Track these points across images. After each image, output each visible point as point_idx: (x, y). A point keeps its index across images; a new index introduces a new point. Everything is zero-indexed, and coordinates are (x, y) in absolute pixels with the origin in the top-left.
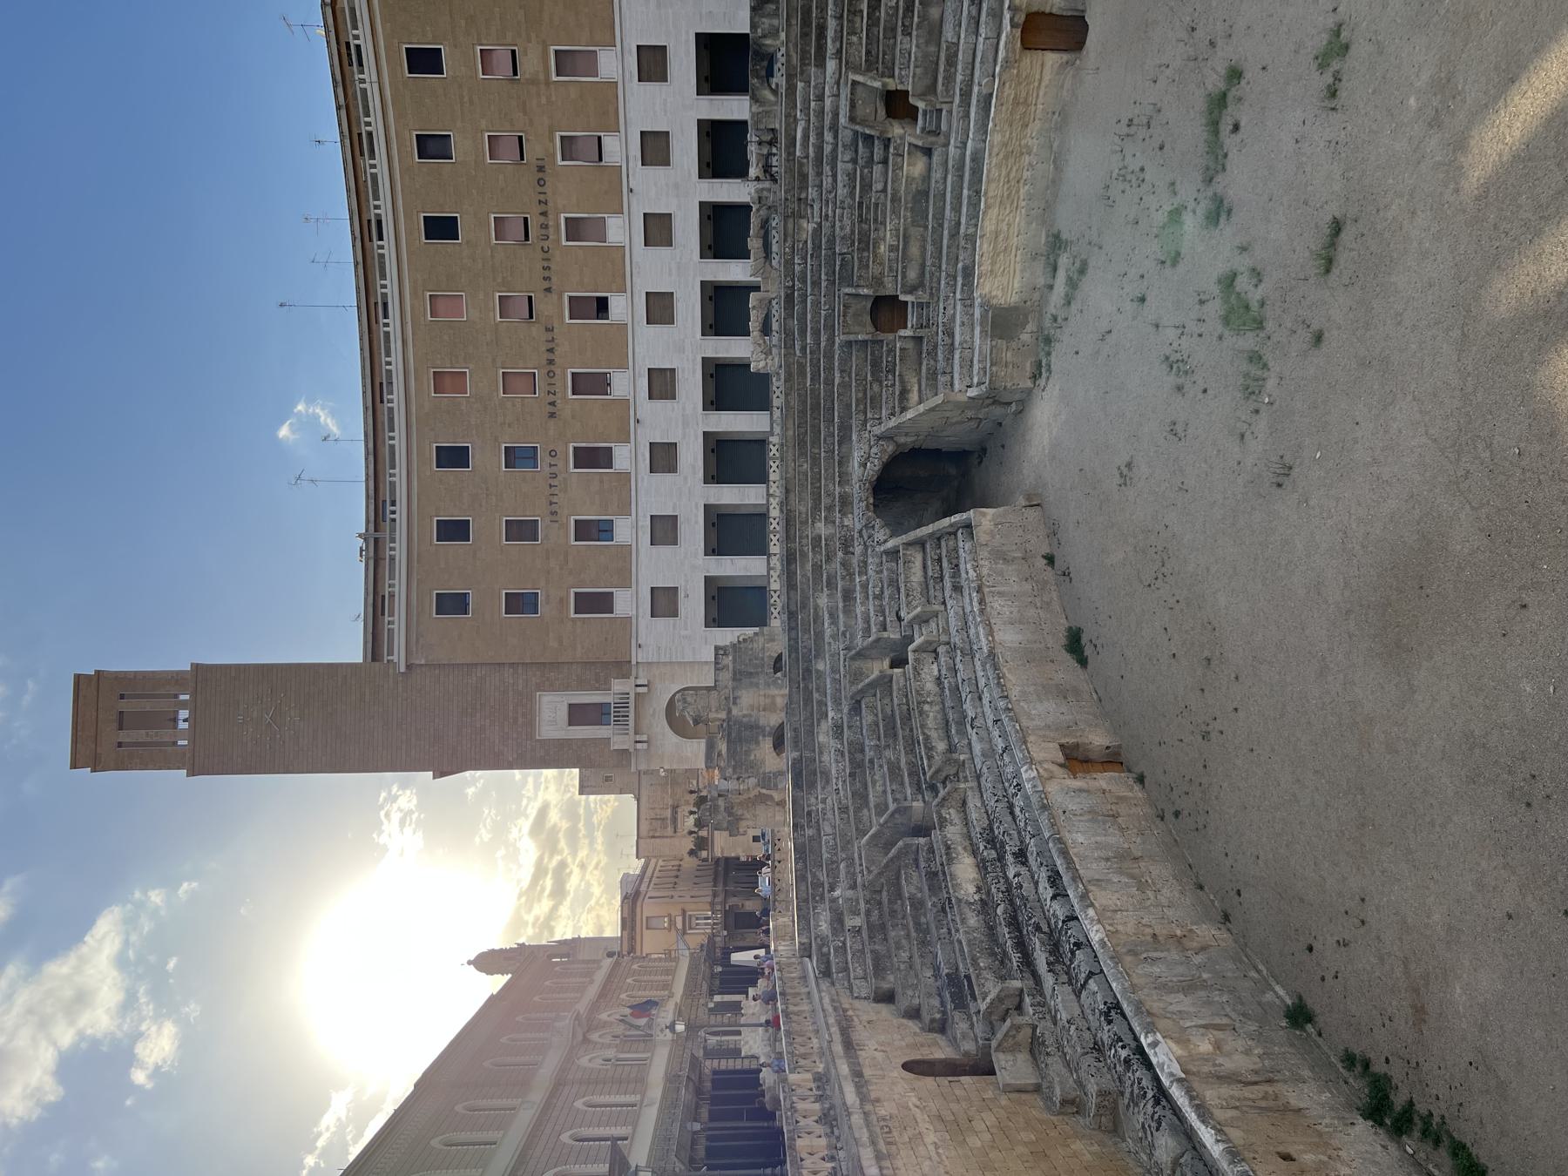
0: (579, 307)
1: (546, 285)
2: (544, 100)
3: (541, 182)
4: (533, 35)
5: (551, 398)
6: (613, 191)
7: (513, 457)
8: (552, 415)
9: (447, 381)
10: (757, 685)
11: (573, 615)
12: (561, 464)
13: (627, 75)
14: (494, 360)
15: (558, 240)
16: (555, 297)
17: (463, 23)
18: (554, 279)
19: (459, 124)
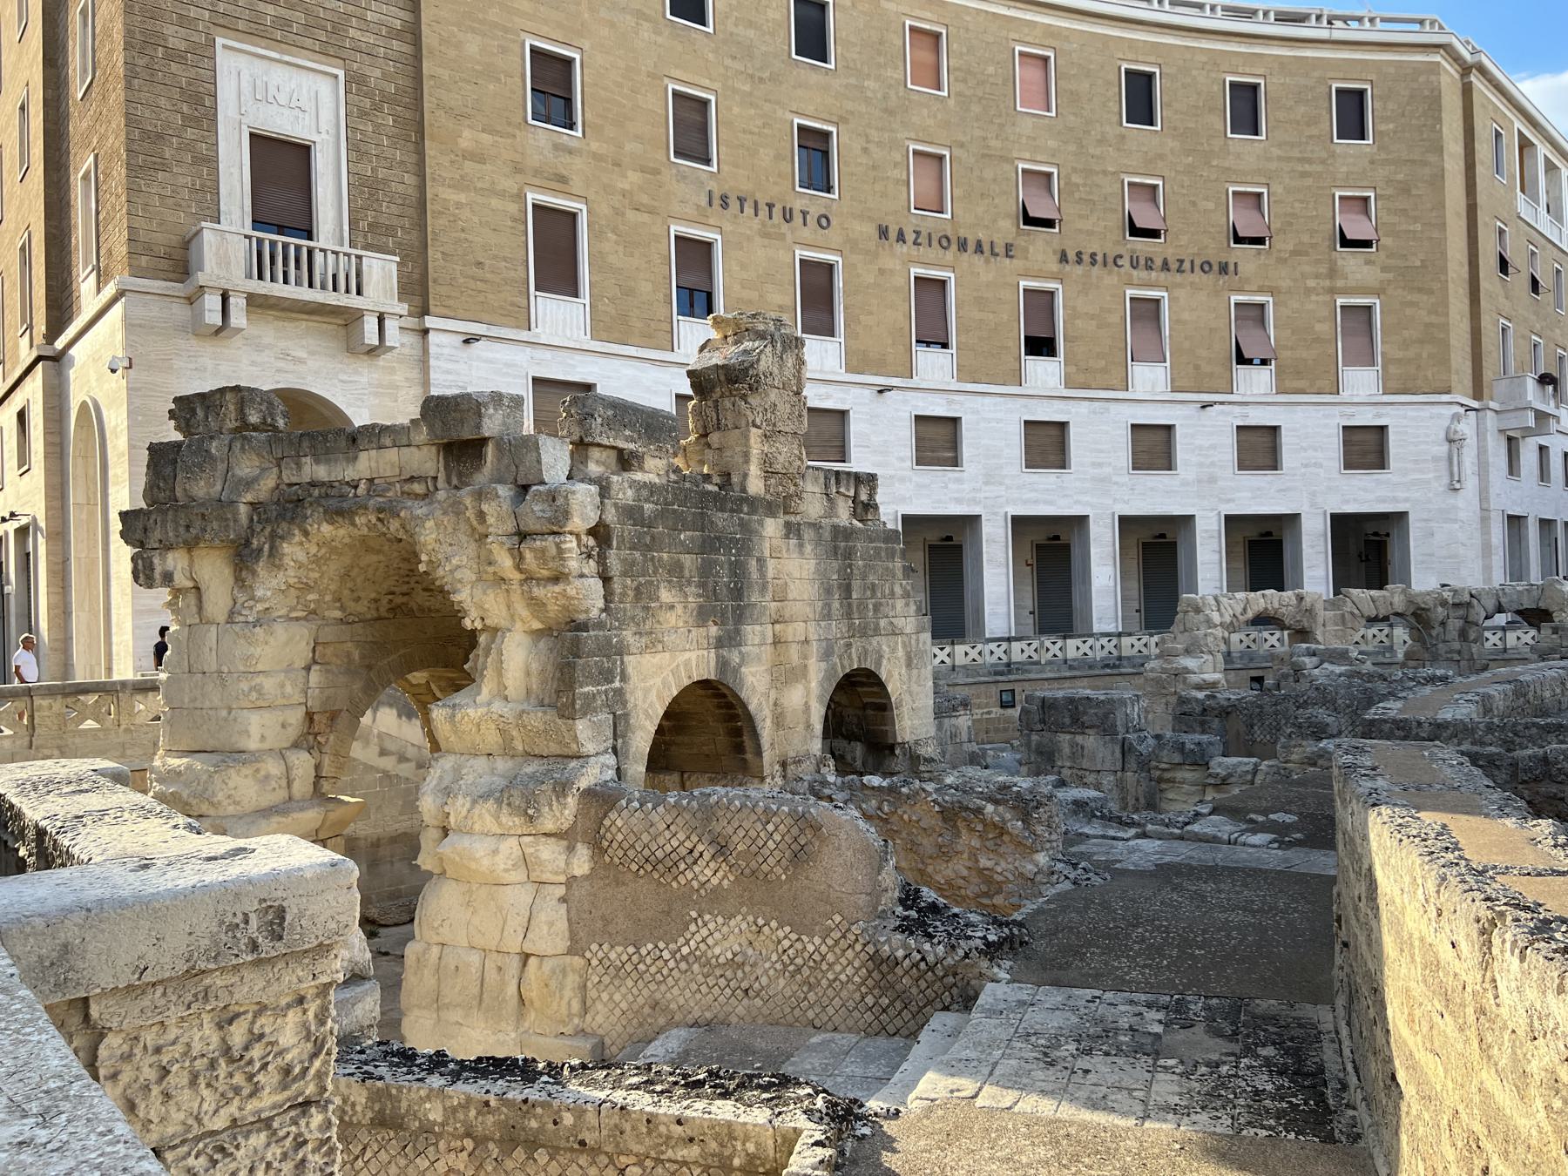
0: (1040, 302)
1: (1071, 256)
2: (1311, 283)
3: (1206, 267)
4: (1390, 276)
5: (910, 237)
6: (1200, 381)
7: (815, 145)
8: (883, 233)
9: (927, 56)
10: (827, 616)
11: (532, 197)
12: (807, 233)
13: (1353, 409)
14: (962, 145)
15: (1131, 285)
16: (1054, 266)
17: (1400, 177)
18: (1079, 270)
19: (1276, 152)
